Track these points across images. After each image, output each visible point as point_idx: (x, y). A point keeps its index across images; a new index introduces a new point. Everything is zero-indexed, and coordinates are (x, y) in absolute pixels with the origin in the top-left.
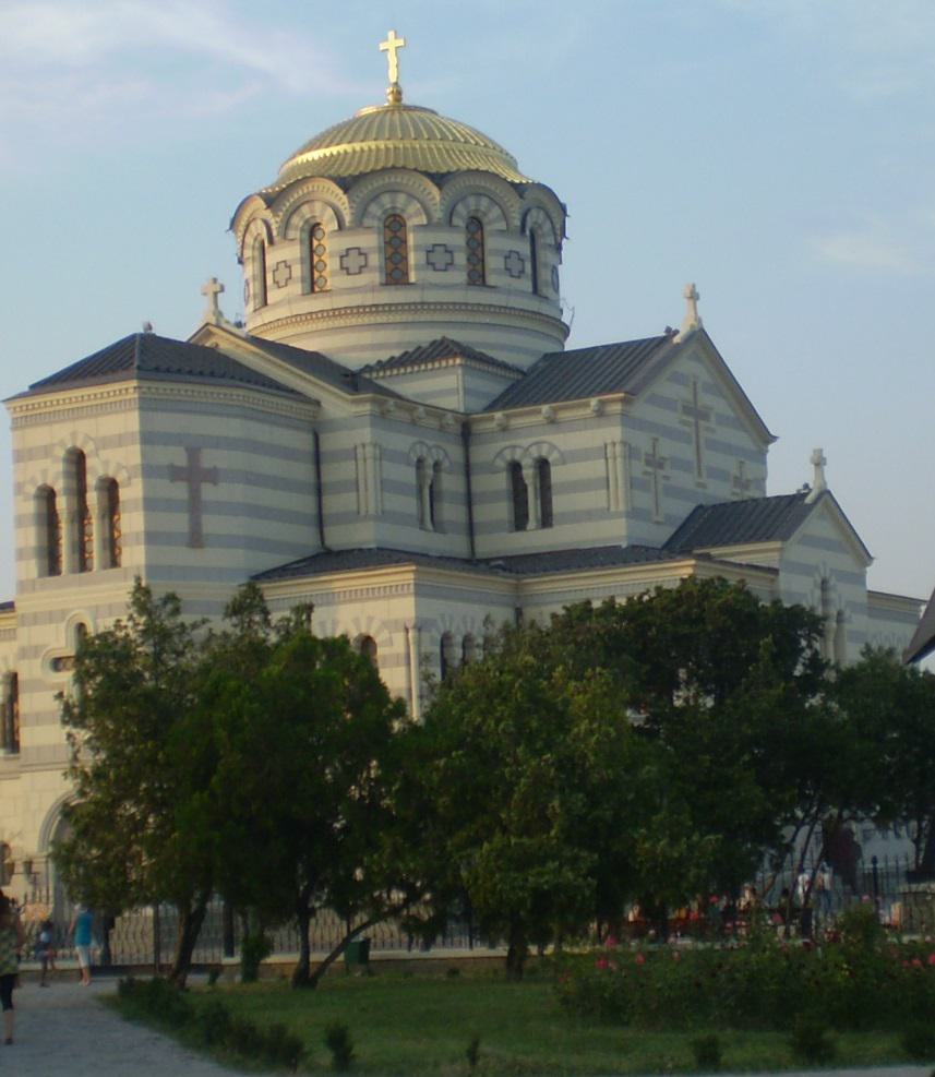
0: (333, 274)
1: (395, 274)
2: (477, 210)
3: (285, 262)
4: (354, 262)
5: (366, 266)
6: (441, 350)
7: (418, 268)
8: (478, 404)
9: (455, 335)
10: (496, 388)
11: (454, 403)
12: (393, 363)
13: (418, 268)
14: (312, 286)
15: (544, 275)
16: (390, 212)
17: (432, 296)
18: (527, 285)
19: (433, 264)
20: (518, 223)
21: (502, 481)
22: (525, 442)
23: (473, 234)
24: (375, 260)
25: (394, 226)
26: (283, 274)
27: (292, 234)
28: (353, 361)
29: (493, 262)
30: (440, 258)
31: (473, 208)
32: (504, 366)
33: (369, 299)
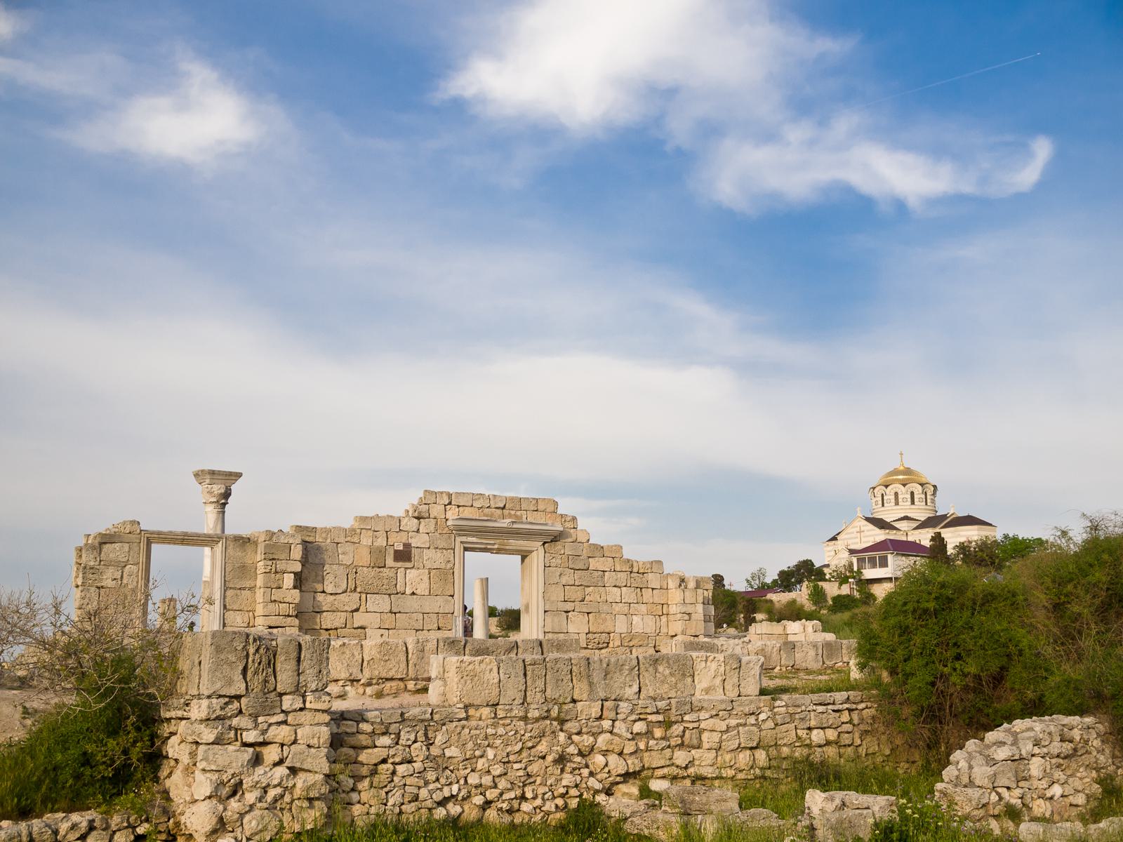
1: (897, 503)
6: (906, 518)
8: (910, 529)
9: (909, 515)
10: (915, 524)
11: (906, 529)
12: (894, 521)
14: (883, 505)
15: (929, 501)
17: (902, 507)
18: (924, 503)
20: (921, 491)
24: (893, 501)
25: (896, 494)
28: (888, 520)
29: (916, 500)
32: (918, 520)
33: (890, 508)
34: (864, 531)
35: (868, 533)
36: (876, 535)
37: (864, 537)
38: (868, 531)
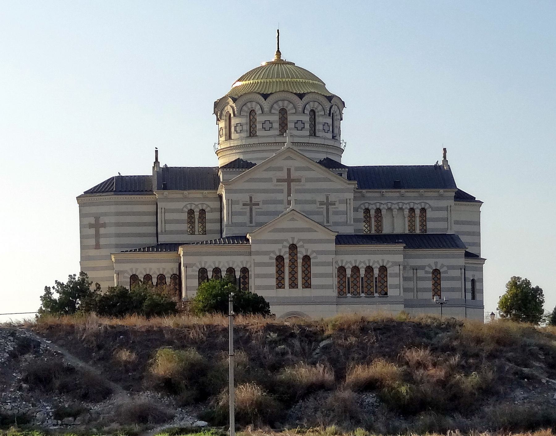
0: (291, 129)
1: (313, 133)
2: (334, 111)
3: (269, 121)
4: (300, 125)
5: (304, 128)
7: (319, 131)
13: (319, 131)
16: (312, 109)
19: (325, 130)
21: (361, 215)
22: (372, 202)
23: (311, 116)
24: (307, 126)
26: (267, 125)
27: (273, 111)
29: (336, 131)
30: (326, 128)
31: (334, 110)
34: (299, 180)
35: (309, 186)
36: (330, 191)
37: (298, 191)
38: (309, 180)
